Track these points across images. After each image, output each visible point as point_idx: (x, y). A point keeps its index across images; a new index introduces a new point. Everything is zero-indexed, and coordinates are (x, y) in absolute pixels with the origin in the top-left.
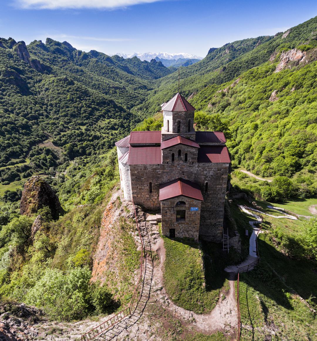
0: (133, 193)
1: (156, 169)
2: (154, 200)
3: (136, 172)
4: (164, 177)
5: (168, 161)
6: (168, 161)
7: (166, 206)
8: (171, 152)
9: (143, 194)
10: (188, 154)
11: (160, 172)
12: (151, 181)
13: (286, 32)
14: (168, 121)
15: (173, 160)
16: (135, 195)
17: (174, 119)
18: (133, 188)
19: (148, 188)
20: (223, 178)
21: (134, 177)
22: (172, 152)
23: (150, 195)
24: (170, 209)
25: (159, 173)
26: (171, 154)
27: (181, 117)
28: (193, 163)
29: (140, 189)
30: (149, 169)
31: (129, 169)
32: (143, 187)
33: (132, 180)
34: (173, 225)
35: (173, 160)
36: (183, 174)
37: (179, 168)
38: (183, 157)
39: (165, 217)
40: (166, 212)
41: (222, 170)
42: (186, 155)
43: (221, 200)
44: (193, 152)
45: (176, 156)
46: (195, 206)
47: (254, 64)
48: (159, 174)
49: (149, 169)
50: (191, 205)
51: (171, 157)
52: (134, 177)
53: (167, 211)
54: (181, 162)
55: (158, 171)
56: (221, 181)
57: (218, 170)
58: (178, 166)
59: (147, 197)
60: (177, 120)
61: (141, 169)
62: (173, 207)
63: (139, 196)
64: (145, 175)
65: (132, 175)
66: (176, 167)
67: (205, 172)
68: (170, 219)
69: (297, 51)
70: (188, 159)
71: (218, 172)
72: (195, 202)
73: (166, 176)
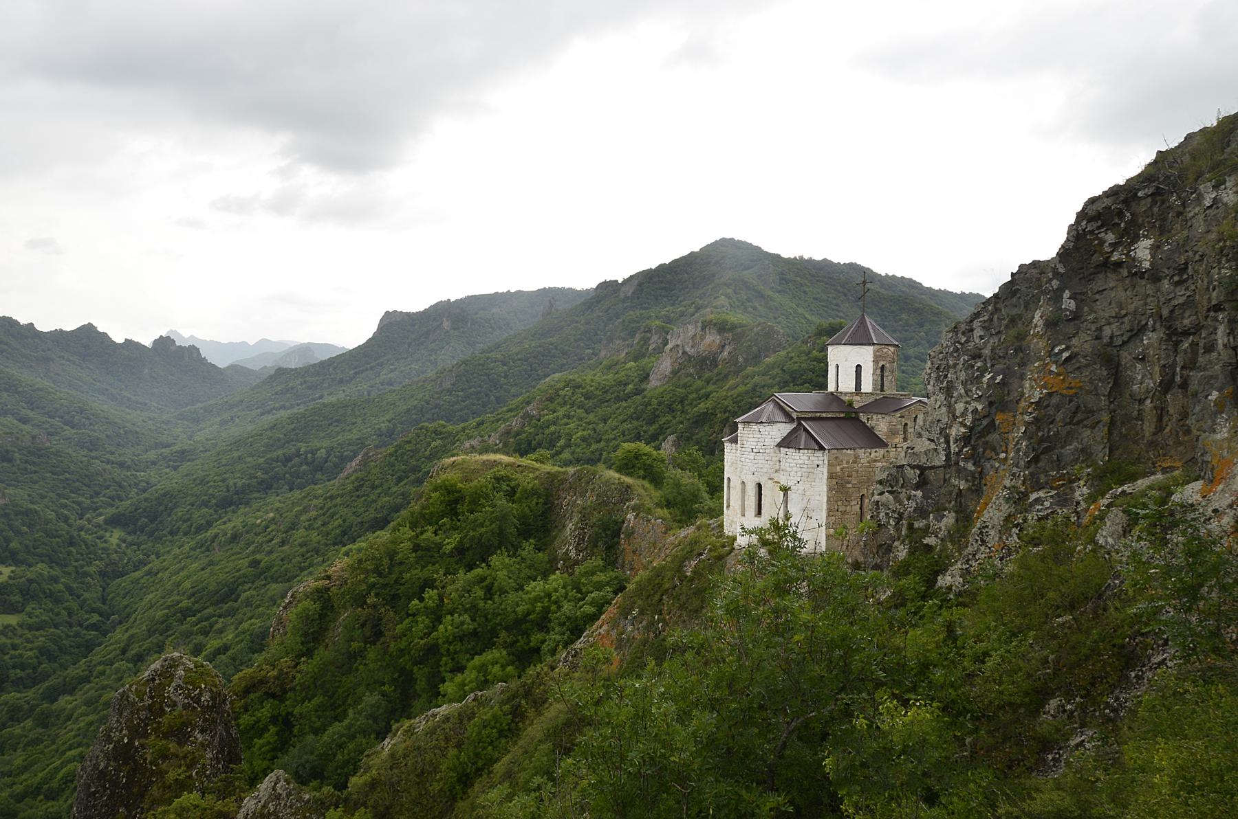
12: (865, 492)
13: (626, 281)
14: (859, 367)
17: (875, 362)
18: (830, 511)
21: (834, 481)
29: (844, 513)
32: (848, 508)
33: (830, 490)
52: (834, 481)
65: (831, 476)
69: (703, 329)
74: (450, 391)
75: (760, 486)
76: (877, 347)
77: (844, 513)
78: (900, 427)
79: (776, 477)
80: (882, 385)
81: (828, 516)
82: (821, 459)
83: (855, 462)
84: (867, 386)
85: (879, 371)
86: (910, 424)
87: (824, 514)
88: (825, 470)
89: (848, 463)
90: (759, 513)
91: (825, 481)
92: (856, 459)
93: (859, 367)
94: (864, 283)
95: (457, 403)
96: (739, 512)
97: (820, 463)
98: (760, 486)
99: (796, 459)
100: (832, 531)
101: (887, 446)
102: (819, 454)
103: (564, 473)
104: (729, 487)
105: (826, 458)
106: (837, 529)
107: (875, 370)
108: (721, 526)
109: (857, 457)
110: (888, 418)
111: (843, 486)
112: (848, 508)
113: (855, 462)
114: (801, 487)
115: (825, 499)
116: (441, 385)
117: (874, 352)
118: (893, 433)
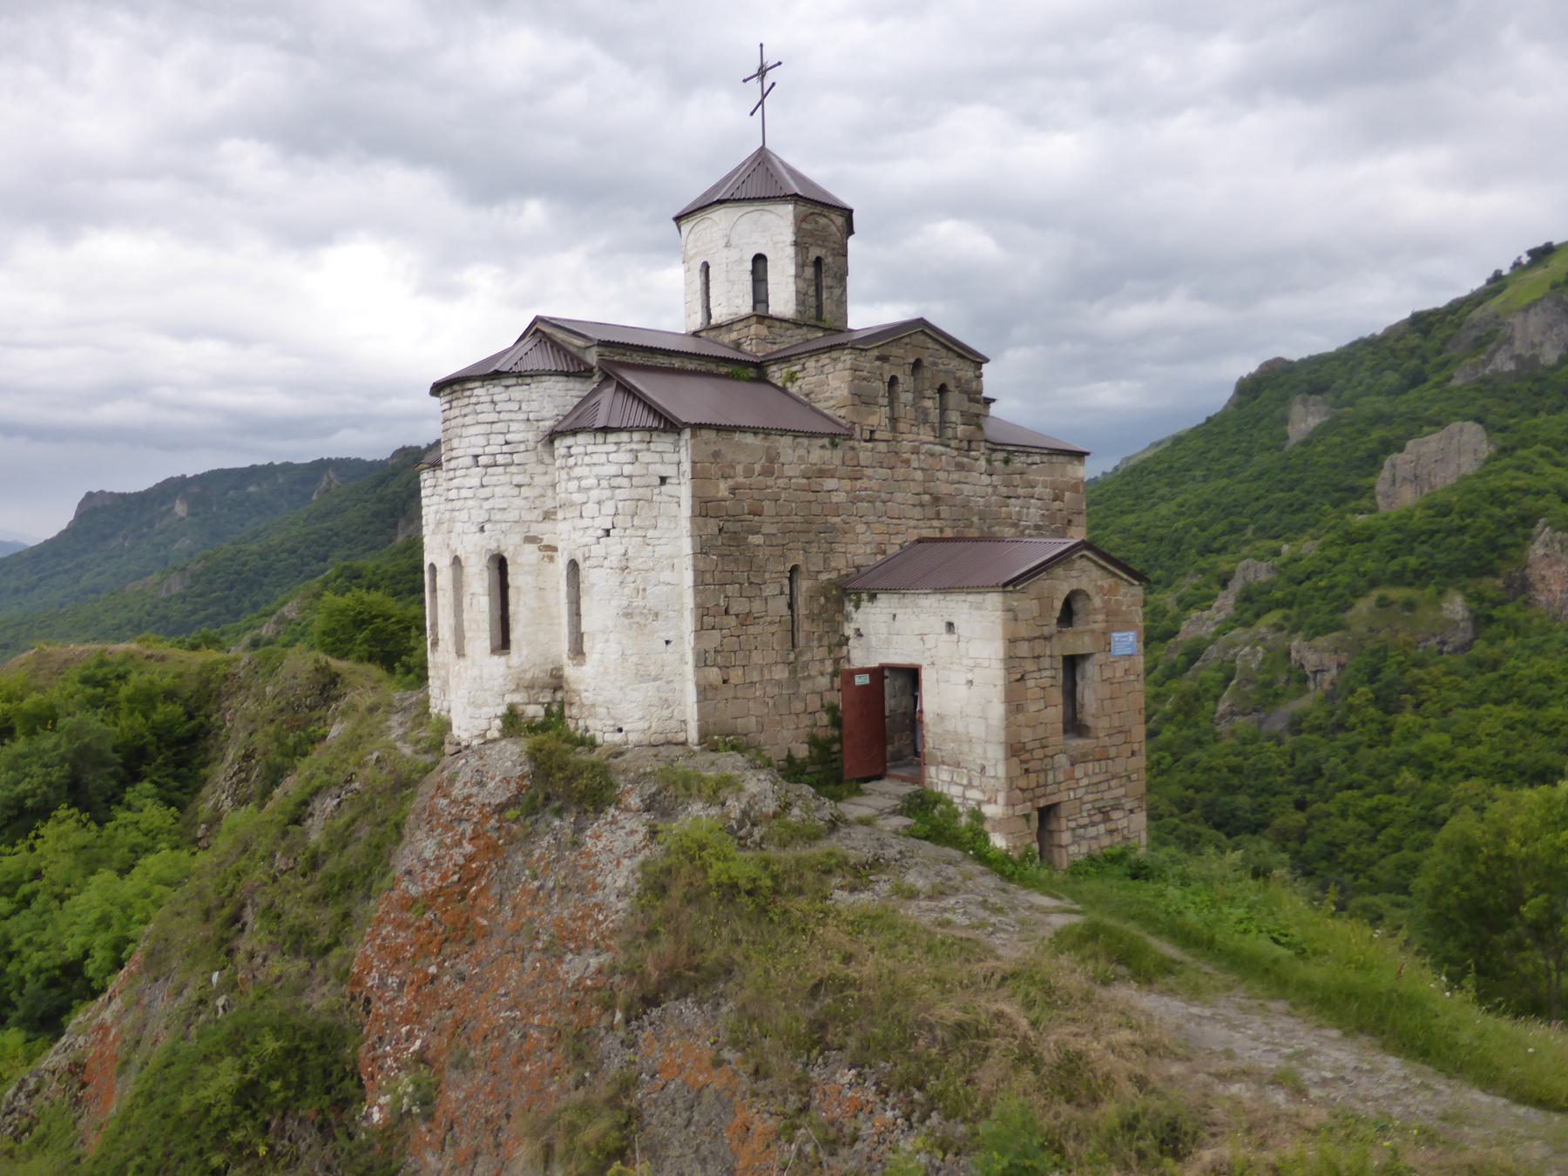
0: (702, 661)
4: (861, 528)
5: (873, 420)
6: (873, 420)
7: (1024, 631)
8: (886, 366)
9: (757, 658)
10: (951, 386)
11: (839, 497)
12: (798, 558)
14: (759, 260)
15: (894, 420)
18: (706, 617)
19: (780, 605)
21: (712, 526)
22: (888, 370)
23: (793, 667)
24: (1039, 647)
25: (835, 498)
27: (825, 239)
29: (745, 619)
30: (788, 470)
32: (757, 606)
36: (938, 517)
37: (919, 475)
42: (942, 389)
47: (325, 559)
48: (836, 510)
49: (788, 470)
50: (1116, 619)
52: (712, 526)
55: (830, 483)
59: (779, 683)
60: (814, 252)
63: (736, 676)
65: (704, 508)
66: (907, 462)
67: (1015, 507)
70: (954, 416)
71: (1057, 505)
74: (183, 598)
75: (500, 565)
76: (804, 209)
77: (745, 619)
78: (880, 387)
79: (547, 532)
80: (819, 308)
81: (701, 629)
82: (675, 458)
83: (768, 472)
84: (783, 298)
85: (809, 272)
86: (905, 380)
87: (688, 623)
88: (685, 491)
89: (749, 472)
90: (503, 643)
91: (685, 524)
93: (759, 260)
94: (762, 72)
95: (193, 612)
96: (452, 649)
97: (669, 471)
98: (500, 565)
99: (598, 462)
100: (714, 674)
102: (663, 443)
103: (228, 663)
104: (434, 590)
105: (685, 456)
106: (718, 660)
107: (801, 266)
108: (425, 703)
109: (772, 458)
110: (847, 358)
111: (737, 540)
112: (757, 606)
113: (768, 472)
114: (615, 546)
115: (688, 578)
116: (168, 590)
117: (799, 221)
118: (862, 399)
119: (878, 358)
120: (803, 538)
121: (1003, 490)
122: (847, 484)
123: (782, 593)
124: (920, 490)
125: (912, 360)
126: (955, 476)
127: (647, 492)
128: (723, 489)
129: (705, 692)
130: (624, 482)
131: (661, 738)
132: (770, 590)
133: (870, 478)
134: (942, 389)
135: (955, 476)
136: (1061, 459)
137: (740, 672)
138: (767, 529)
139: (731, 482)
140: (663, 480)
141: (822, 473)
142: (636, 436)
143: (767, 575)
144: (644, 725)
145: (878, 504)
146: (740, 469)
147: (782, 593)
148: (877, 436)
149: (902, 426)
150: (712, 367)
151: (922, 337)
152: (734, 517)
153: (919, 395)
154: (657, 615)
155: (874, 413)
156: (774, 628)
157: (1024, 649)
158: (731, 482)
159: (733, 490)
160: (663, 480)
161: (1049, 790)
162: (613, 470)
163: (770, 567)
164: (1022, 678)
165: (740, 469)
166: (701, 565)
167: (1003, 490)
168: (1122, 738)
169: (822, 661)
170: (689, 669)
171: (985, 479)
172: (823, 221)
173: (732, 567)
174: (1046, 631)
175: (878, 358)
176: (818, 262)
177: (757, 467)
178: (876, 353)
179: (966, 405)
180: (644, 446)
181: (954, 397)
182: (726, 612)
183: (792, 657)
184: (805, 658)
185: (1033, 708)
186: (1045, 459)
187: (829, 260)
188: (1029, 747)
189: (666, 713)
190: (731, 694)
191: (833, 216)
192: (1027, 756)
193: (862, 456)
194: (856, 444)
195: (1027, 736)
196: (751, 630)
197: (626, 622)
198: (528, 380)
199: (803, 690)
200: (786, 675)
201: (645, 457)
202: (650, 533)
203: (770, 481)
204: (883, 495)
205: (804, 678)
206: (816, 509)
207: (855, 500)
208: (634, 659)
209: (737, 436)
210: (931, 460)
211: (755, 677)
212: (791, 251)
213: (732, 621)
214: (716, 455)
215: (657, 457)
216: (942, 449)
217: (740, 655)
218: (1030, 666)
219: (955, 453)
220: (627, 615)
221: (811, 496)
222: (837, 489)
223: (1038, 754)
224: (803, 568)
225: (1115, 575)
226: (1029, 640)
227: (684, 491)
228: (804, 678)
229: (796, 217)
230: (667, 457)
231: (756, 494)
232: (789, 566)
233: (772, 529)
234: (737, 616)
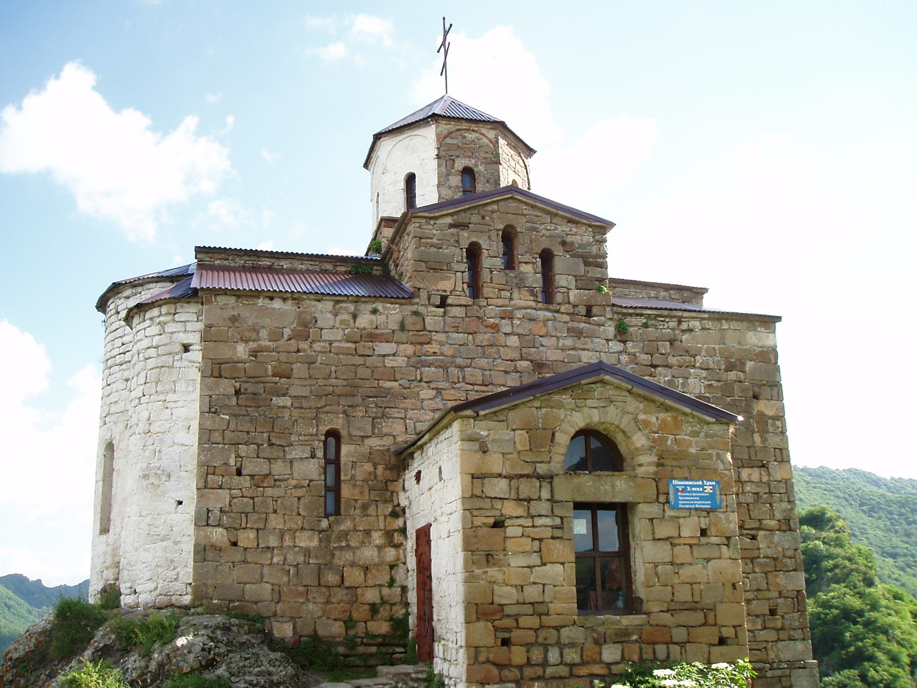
0: (204, 520)
1: (373, 337)
2: (354, 577)
3: (242, 350)
5: (446, 285)
7: (495, 463)
8: (465, 234)
9: (275, 522)
10: (558, 251)
11: (400, 361)
12: (338, 423)
14: (410, 180)
15: (475, 288)
16: (218, 535)
19: (312, 469)
20: (761, 414)
21: (227, 387)
23: (325, 535)
24: (527, 488)
25: (389, 363)
26: (465, 244)
28: (589, 314)
29: (258, 481)
30: (327, 335)
31: (194, 339)
32: (278, 468)
33: (211, 408)
34: (553, 656)
35: (475, 288)
37: (514, 341)
38: (530, 271)
39: (493, 572)
40: (499, 524)
41: (749, 365)
42: (547, 257)
43: (781, 579)
44: (581, 246)
45: (491, 261)
46: (698, 469)
49: (327, 335)
51: (464, 267)
52: (227, 387)
53: (510, 509)
54: (522, 299)
55: (384, 348)
56: (757, 438)
57: (730, 368)
58: (506, 326)
59: (307, 552)
60: (460, 164)
61: (276, 335)
62: (550, 478)
63: (247, 538)
64: (299, 369)
65: (215, 370)
66: (495, 328)
68: (532, 593)
70: (562, 281)
71: (732, 375)
72: (691, 437)
73: (439, 391)
76: (445, 127)
78: (457, 256)
81: (204, 487)
89: (276, 335)
92: (305, 329)
93: (410, 180)
101: (411, 297)
115: (192, 438)
117: (441, 140)
119: (452, 226)
120: (343, 401)
121: (644, 358)
122: (409, 349)
123: (313, 456)
124: (516, 355)
125: (501, 227)
126: (569, 342)
127: (168, 360)
128: (242, 350)
129: (203, 552)
130: (152, 352)
131: (163, 600)
132: (295, 453)
133: (441, 344)
134: (547, 257)
135: (569, 342)
136: (734, 325)
137: (252, 535)
138: (293, 391)
139: (252, 345)
140: (186, 348)
141: (373, 337)
142: (164, 309)
143: (294, 438)
144: (151, 586)
145: (453, 371)
146: (264, 333)
147: (313, 456)
148: (449, 301)
149: (486, 291)
150: (329, 267)
151: (513, 205)
152: (255, 379)
153: (510, 263)
154: (169, 476)
155: (449, 278)
156: (300, 492)
157: (500, 487)
158: (252, 345)
159: (254, 353)
160: (186, 348)
161: (550, 671)
162: (145, 343)
163: (298, 428)
164: (499, 524)
165: (264, 333)
166: (208, 424)
167: (644, 358)
168: (699, 617)
169: (368, 533)
170: (191, 529)
171: (618, 346)
172: (470, 136)
173: (247, 427)
174: (542, 469)
175: (452, 226)
176: (468, 172)
177: (287, 332)
178: (449, 220)
179: (582, 269)
180: (169, 318)
181: (561, 262)
182: (239, 473)
183: (325, 523)
184: (346, 525)
185: (517, 561)
186: (709, 324)
187: (480, 168)
188: (508, 610)
189: (172, 574)
190: (238, 557)
191: (484, 131)
192: (508, 622)
193: (428, 320)
194: (422, 309)
195: (506, 595)
196: (269, 492)
197: (145, 483)
198: (139, 289)
199: (337, 561)
200: (315, 543)
201: (170, 328)
202: (170, 397)
203: (304, 345)
204: (459, 361)
205: (341, 548)
206: (362, 372)
207: (417, 362)
208: (148, 520)
209: (260, 302)
210: (531, 325)
211: (273, 542)
212: (434, 163)
213: (245, 482)
214: (234, 319)
215: (180, 327)
216: (549, 315)
217: (253, 517)
218: (510, 509)
219: (566, 318)
220: (146, 476)
221: (359, 360)
222: (395, 355)
223: (534, 622)
224: (344, 433)
225: (667, 409)
226: (510, 477)
227: (196, 355)
228: (341, 548)
229: (438, 135)
230: (189, 326)
231: (283, 357)
232: (324, 429)
233: (305, 392)
234: (252, 476)
